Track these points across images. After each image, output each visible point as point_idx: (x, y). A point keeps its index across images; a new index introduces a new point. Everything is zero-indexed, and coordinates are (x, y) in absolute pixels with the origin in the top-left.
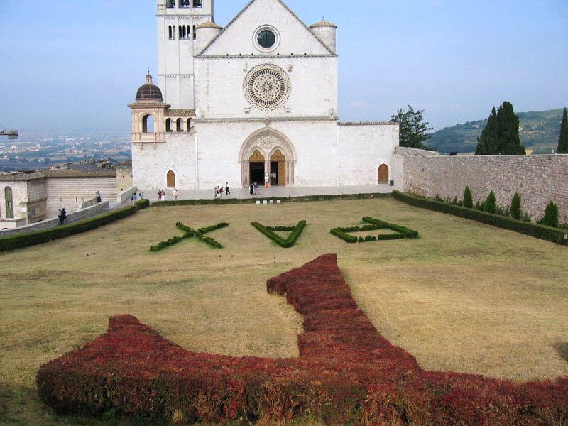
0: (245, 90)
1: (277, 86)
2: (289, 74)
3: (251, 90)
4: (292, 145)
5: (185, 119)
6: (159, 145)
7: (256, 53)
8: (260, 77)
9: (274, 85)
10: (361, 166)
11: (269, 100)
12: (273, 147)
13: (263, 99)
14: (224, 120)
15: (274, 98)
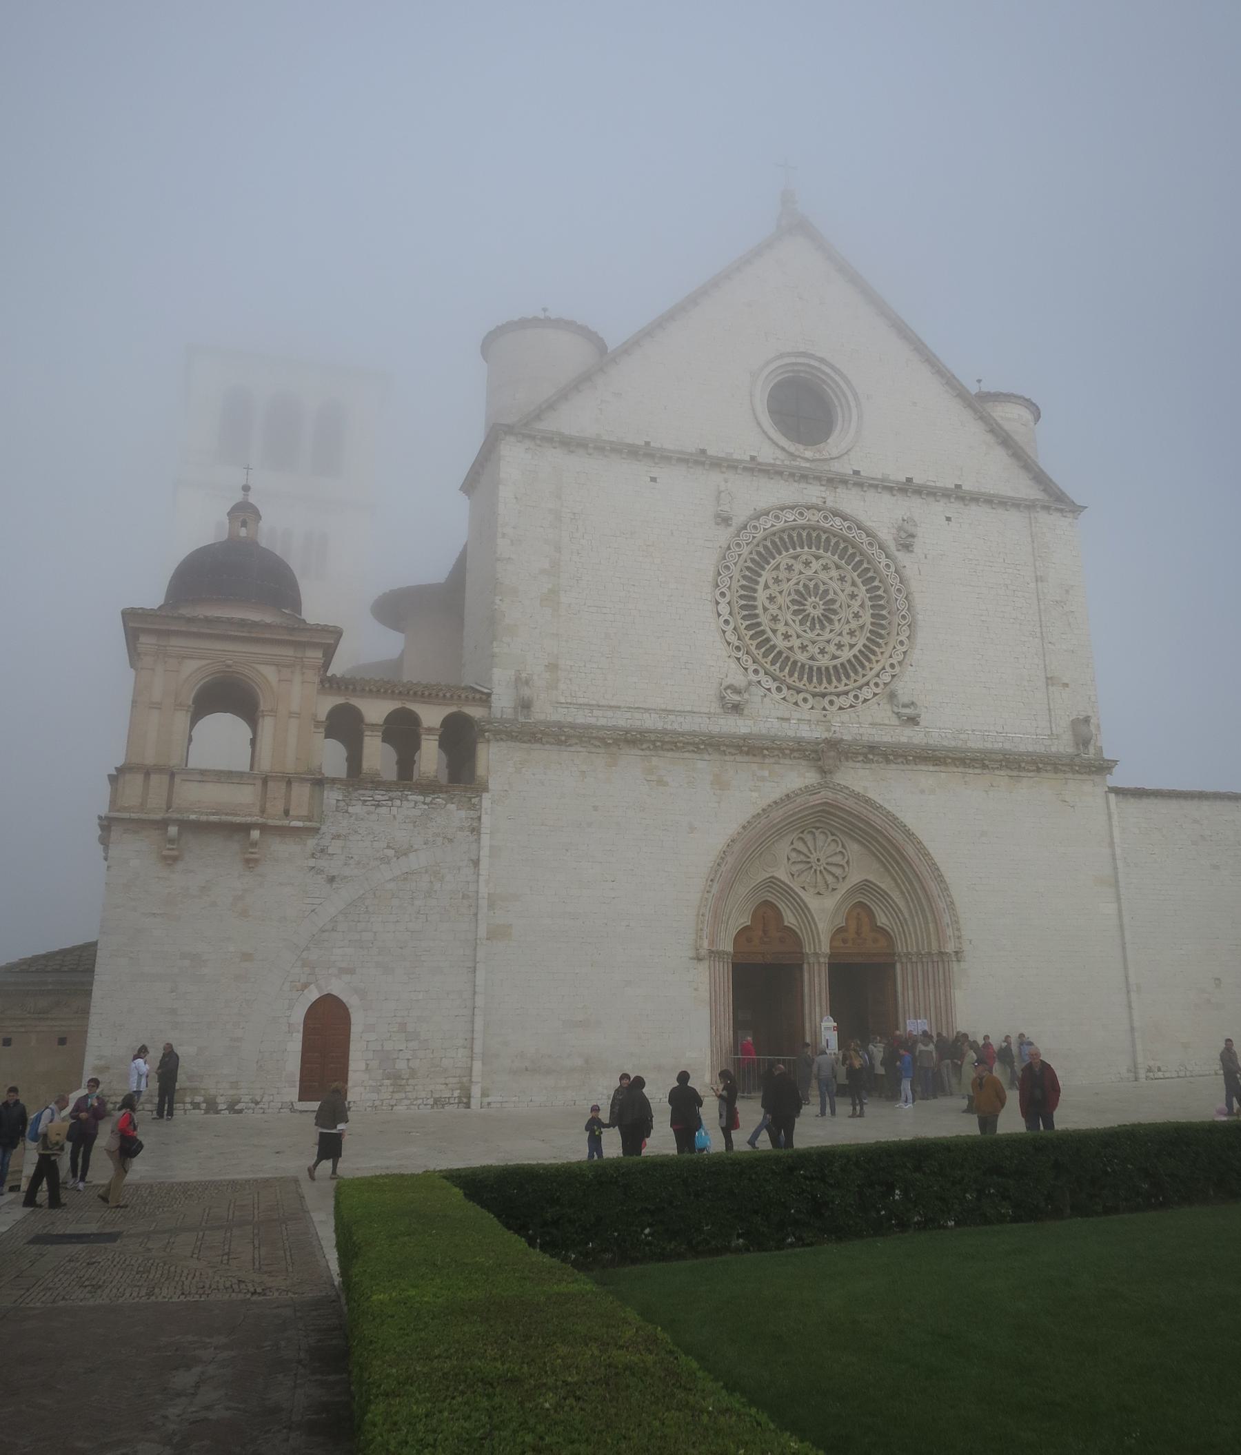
0: (724, 609)
1: (856, 605)
2: (901, 556)
3: (749, 609)
4: (940, 879)
5: (431, 716)
6: (281, 848)
7: (767, 454)
8: (783, 559)
9: (843, 597)
10: (1218, 981)
11: (824, 661)
12: (843, 888)
13: (802, 657)
14: (633, 739)
15: (846, 654)
